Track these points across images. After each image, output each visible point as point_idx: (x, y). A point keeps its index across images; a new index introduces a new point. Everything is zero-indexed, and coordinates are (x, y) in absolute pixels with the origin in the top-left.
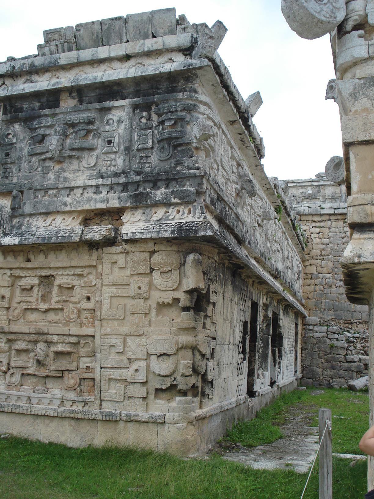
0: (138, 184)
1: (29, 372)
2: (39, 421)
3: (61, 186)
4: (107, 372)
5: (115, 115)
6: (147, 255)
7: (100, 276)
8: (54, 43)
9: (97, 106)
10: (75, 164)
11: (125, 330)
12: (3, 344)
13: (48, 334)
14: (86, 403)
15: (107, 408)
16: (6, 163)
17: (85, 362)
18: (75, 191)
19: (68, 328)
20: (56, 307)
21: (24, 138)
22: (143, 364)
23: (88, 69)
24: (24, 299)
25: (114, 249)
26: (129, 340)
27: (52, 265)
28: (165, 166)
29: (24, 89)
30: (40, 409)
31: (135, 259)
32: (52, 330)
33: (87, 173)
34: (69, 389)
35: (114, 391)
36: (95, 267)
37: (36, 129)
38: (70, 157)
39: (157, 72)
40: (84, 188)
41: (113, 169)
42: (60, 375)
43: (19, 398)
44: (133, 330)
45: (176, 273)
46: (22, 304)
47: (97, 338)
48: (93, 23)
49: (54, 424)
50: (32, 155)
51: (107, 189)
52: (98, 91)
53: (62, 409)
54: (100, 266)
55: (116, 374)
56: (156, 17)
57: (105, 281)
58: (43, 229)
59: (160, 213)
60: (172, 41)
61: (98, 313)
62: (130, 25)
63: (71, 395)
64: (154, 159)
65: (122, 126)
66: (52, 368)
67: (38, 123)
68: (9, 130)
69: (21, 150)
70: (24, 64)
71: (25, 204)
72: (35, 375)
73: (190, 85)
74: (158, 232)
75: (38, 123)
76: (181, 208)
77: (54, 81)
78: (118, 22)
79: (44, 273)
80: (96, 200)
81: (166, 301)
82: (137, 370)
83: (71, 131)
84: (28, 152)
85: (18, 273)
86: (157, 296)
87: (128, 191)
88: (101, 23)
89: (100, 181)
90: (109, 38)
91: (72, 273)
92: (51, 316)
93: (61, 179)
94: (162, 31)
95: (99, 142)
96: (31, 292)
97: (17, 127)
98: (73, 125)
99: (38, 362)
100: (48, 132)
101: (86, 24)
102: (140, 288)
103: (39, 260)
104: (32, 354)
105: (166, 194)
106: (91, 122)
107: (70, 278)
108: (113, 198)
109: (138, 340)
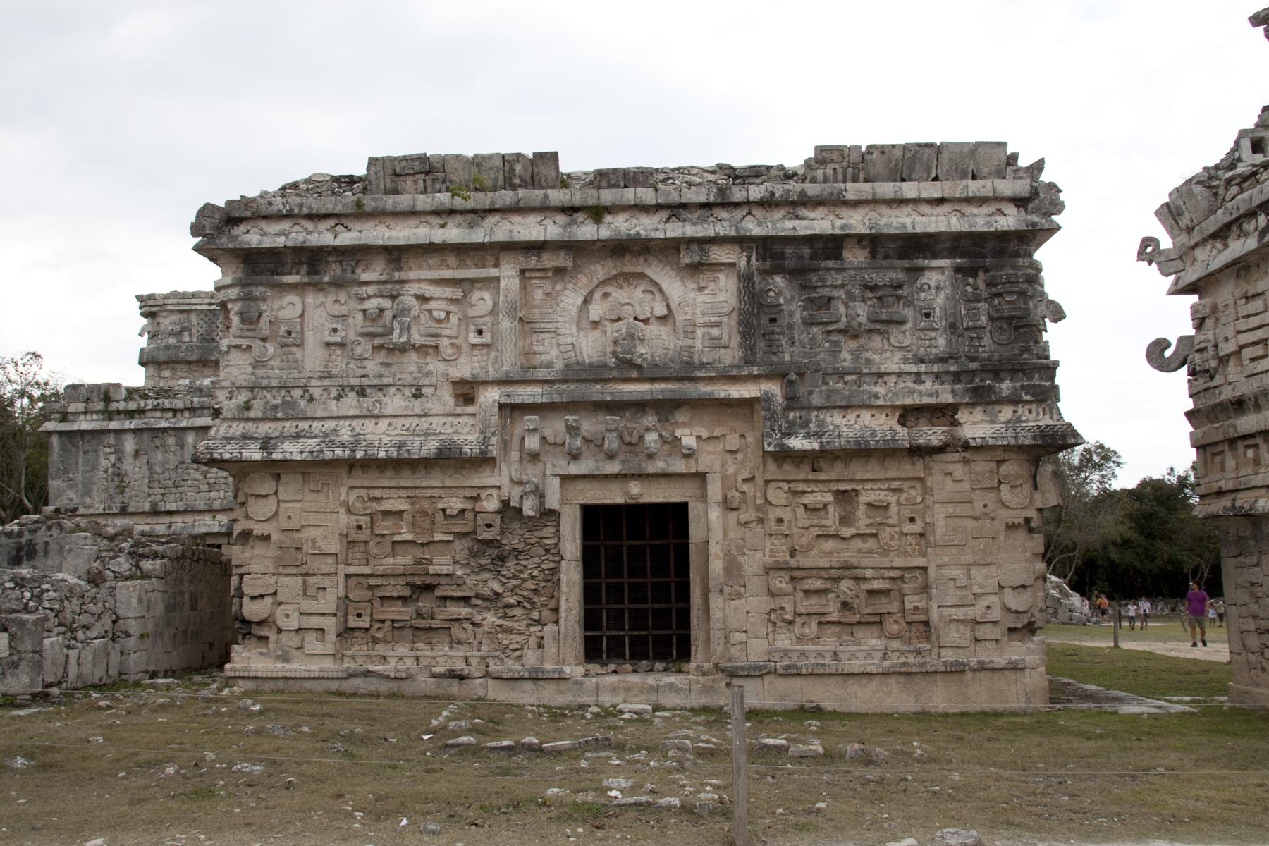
0: (973, 373)
1: (830, 619)
2: (851, 681)
3: (865, 371)
4: (946, 612)
5: (932, 278)
6: (994, 465)
7: (926, 490)
8: (832, 165)
9: (906, 263)
10: (877, 341)
11: (967, 558)
12: (783, 585)
13: (856, 568)
14: (919, 652)
15: (948, 655)
16: (773, 333)
17: (911, 602)
18: (886, 378)
19: (886, 559)
20: (868, 531)
21: (793, 298)
22: (994, 599)
23: (884, 210)
24: (816, 522)
25: (948, 457)
26: (973, 571)
27: (858, 477)
28: (1007, 352)
29: (794, 229)
30: (856, 665)
31: (978, 469)
32: (865, 562)
33: (898, 356)
34: (892, 637)
35: (955, 635)
36: (921, 479)
37: (816, 287)
38: (870, 331)
39: (992, 229)
40: (900, 375)
41: (934, 351)
42: (877, 622)
43: (820, 654)
44: (978, 558)
45: (1027, 487)
46: (812, 530)
47: (932, 571)
48: (893, 146)
49: (874, 684)
50: (808, 323)
51: (932, 377)
52: (900, 243)
53: (887, 663)
54: (930, 479)
55: (959, 614)
56: (981, 151)
57: (938, 497)
58: (845, 429)
59: (1007, 413)
60: (1007, 187)
61: (932, 539)
62: (945, 156)
63: (896, 644)
64: (987, 340)
65: (942, 294)
66: (865, 612)
67: (820, 279)
68: (768, 284)
69: (791, 314)
70: (789, 191)
71: (811, 392)
72: (839, 623)
73: (1024, 247)
74: (1016, 437)
75: (820, 279)
76: (1033, 407)
77: (839, 223)
78: (927, 150)
79: (842, 487)
80: (920, 393)
81: (1016, 521)
82: (988, 607)
83: (870, 295)
84: (803, 318)
85: (801, 487)
86: (1006, 516)
87: (959, 382)
88: (905, 147)
89: (923, 368)
90: (911, 170)
91: (886, 486)
92: (857, 544)
93: (863, 361)
94: (986, 170)
95: (908, 313)
96: (822, 513)
97: (779, 280)
98: (873, 288)
99: (845, 605)
100: (836, 293)
101: (883, 146)
102: (985, 506)
103: (834, 471)
104: (832, 595)
105: (1015, 388)
106: (900, 287)
107: (882, 493)
108: (944, 391)
109: (985, 570)
